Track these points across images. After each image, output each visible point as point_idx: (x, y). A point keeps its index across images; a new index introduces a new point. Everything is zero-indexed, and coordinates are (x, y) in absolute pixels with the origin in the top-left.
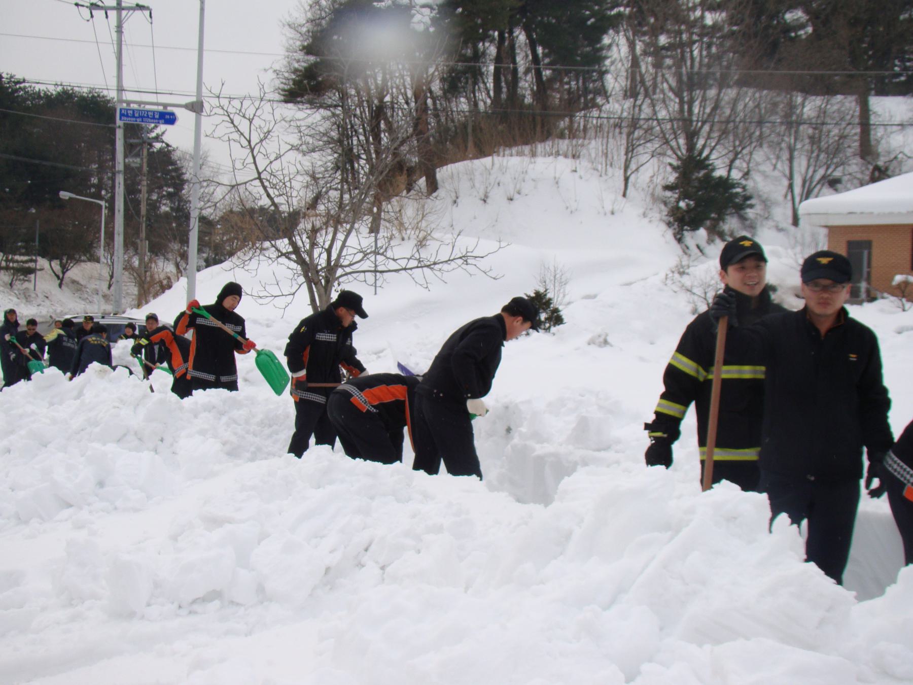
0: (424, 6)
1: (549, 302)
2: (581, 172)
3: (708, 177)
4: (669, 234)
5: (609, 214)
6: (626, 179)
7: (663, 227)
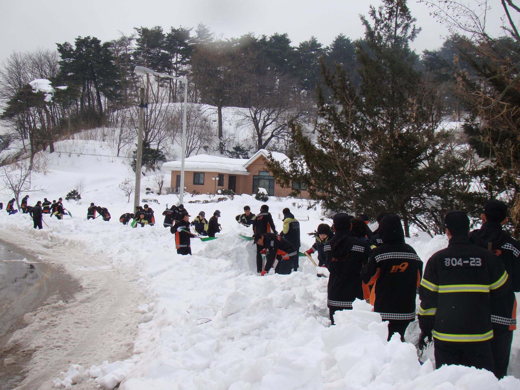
0: (49, 93)
1: (77, 193)
2: (103, 147)
3: (149, 149)
4: (131, 169)
5: (111, 162)
6: (119, 150)
7: (130, 166)
